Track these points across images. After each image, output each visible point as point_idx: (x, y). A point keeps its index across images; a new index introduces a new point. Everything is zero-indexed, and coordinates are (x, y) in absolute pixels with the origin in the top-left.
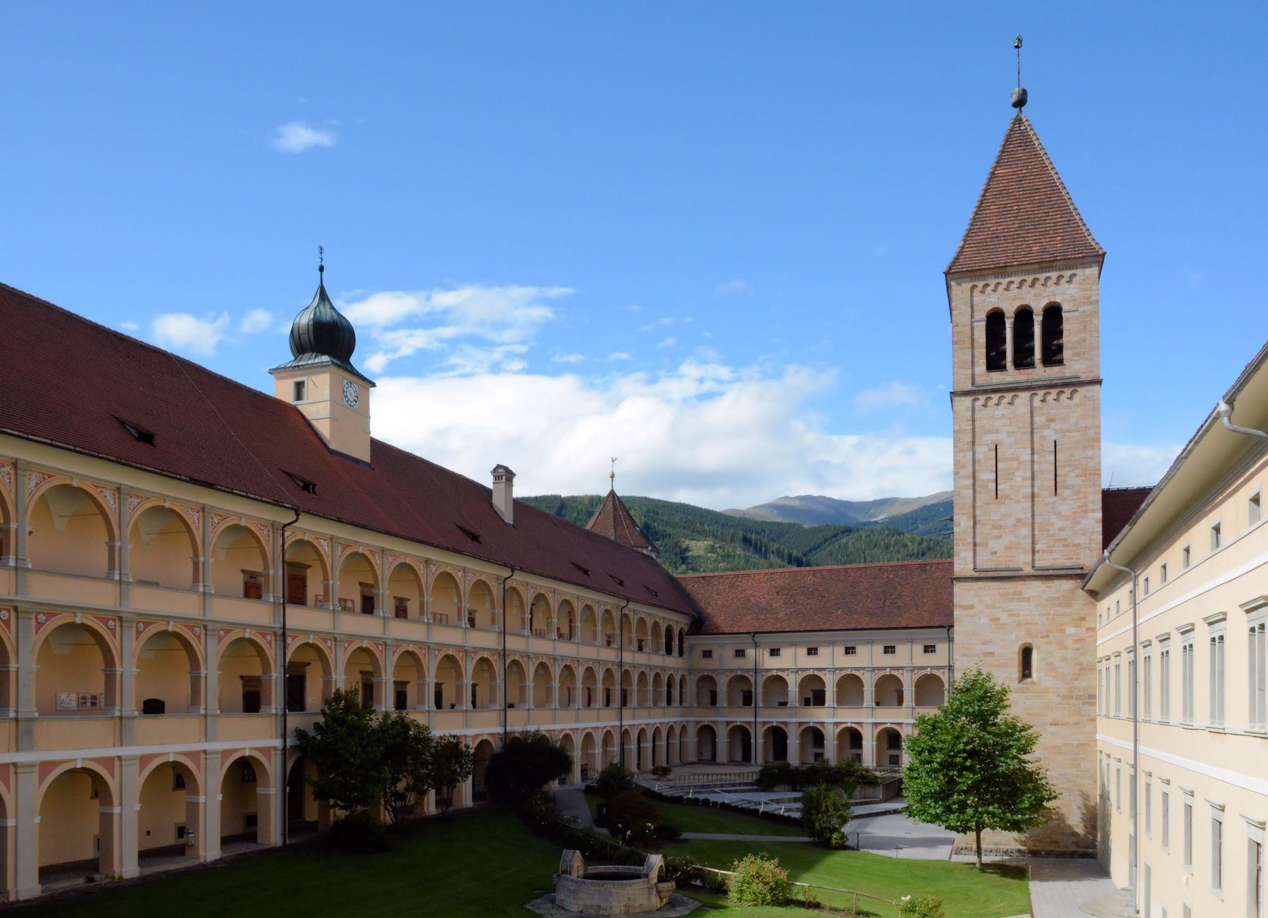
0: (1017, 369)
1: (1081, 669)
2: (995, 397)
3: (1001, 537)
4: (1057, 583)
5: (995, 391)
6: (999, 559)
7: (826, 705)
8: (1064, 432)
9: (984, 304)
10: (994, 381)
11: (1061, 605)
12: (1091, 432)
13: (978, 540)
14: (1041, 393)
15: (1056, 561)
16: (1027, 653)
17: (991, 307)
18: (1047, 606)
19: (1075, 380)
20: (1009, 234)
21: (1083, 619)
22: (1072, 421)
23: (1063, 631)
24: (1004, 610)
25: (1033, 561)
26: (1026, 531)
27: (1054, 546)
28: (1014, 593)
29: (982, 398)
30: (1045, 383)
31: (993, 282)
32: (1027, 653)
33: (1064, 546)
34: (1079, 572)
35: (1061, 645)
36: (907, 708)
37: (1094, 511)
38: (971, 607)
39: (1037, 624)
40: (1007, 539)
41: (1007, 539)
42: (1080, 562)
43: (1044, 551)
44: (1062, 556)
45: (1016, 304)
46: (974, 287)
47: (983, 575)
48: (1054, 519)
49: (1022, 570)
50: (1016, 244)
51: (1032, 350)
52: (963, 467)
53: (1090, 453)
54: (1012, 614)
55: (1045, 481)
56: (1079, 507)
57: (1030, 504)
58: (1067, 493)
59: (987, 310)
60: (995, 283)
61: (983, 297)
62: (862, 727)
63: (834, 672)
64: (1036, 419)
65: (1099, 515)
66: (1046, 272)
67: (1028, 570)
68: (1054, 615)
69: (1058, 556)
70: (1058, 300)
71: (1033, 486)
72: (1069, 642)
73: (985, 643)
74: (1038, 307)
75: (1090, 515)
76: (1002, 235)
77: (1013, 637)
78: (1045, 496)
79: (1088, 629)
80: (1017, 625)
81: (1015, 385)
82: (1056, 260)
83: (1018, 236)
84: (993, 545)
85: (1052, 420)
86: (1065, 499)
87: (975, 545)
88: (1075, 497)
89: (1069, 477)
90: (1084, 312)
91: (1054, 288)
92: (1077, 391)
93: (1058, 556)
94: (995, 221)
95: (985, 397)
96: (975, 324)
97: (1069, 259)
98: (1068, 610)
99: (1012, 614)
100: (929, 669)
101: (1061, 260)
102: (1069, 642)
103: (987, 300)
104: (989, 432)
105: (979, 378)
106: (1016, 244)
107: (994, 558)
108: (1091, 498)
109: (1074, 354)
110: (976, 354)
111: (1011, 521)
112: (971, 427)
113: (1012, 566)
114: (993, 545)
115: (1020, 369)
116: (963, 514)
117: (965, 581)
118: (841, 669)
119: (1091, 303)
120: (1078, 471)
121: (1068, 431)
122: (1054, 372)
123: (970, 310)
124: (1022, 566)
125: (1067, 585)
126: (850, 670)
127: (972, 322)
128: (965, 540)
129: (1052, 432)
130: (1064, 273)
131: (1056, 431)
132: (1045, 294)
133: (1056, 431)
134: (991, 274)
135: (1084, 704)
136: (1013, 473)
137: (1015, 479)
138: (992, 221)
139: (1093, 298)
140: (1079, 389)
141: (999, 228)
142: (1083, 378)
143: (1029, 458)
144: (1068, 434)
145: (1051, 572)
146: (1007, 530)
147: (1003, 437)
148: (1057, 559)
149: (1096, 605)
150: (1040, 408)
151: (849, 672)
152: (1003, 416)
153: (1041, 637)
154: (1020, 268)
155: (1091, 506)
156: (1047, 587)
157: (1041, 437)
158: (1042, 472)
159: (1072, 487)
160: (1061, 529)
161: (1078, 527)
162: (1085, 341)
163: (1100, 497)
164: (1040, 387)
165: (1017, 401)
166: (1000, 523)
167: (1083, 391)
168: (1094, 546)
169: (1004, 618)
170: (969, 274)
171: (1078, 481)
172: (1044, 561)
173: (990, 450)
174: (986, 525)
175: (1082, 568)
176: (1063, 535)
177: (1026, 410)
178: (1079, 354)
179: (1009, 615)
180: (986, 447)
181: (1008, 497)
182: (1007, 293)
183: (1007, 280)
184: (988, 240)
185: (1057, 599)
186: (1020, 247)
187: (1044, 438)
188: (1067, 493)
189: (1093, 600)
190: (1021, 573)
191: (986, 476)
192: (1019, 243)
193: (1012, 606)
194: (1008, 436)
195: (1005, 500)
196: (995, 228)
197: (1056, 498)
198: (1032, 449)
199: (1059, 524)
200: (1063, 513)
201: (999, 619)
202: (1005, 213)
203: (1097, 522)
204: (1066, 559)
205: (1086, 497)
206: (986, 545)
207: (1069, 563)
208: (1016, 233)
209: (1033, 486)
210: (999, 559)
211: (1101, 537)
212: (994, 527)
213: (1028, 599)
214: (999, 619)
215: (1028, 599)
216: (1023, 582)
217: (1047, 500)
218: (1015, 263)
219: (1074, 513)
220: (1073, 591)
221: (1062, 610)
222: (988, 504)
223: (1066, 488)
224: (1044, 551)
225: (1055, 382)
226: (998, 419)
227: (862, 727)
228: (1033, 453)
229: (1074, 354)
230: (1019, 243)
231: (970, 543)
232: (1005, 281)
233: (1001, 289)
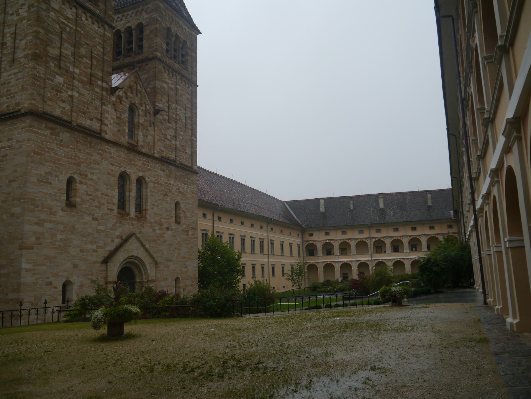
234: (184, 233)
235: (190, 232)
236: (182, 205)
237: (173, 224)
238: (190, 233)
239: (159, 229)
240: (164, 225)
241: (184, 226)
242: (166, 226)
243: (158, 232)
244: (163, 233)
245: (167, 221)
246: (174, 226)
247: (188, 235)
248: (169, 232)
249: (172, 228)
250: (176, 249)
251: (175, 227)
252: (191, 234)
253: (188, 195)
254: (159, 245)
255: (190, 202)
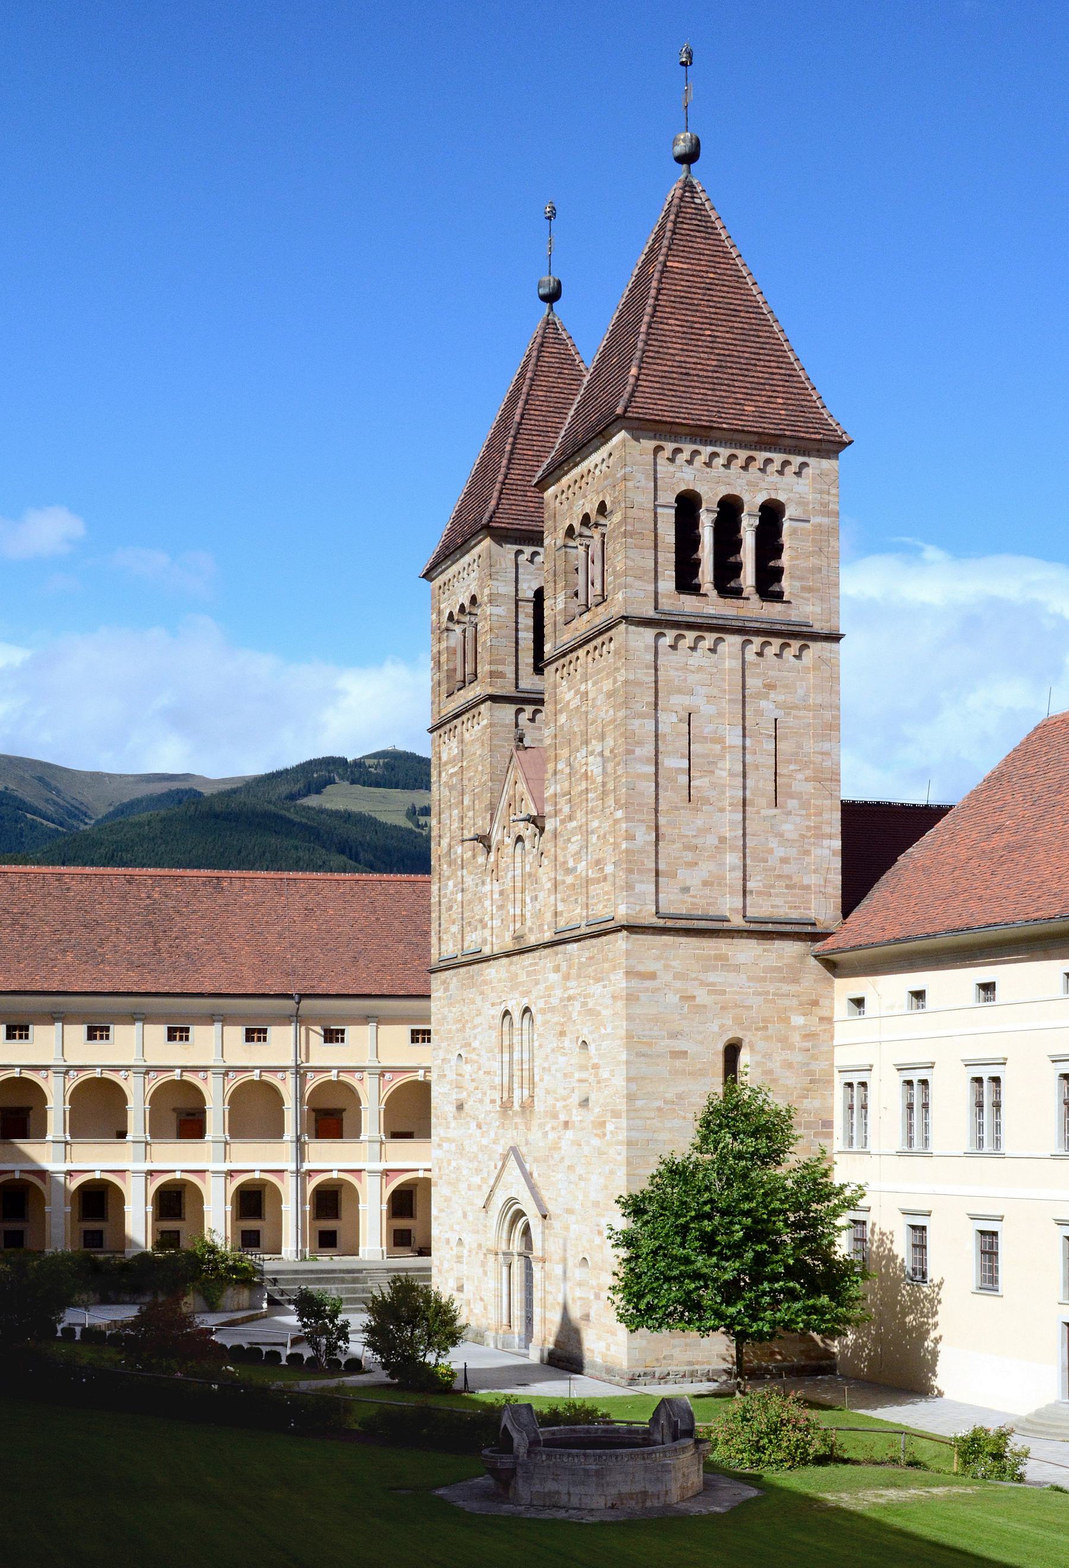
0: (721, 597)
1: (812, 1081)
2: (691, 635)
3: (696, 864)
4: (778, 944)
5: (691, 626)
6: (694, 900)
7: (49, 1137)
8: (788, 708)
9: (674, 480)
10: (688, 609)
11: (783, 980)
12: (828, 715)
13: (662, 867)
14: (758, 641)
15: (775, 910)
16: (732, 1052)
17: (683, 488)
18: (763, 979)
19: (805, 629)
20: (705, 374)
21: (815, 1003)
22: (801, 692)
23: (787, 1020)
24: (703, 984)
25: (744, 907)
26: (733, 859)
27: (773, 886)
28: (718, 957)
29: (670, 635)
30: (763, 626)
31: (688, 448)
32: (732, 1052)
33: (787, 887)
34: (809, 929)
35: (784, 1041)
36: (134, 1142)
37: (830, 837)
38: (652, 976)
39: (749, 1008)
40: (706, 869)
41: (706, 869)
42: (812, 914)
43: (759, 893)
44: (785, 902)
45: (722, 491)
46: (658, 449)
47: (670, 924)
48: (773, 843)
49: (729, 921)
50: (718, 393)
51: (738, 567)
52: (640, 743)
53: (826, 746)
54: (714, 990)
55: (760, 782)
56: (808, 828)
57: (740, 816)
58: (792, 804)
59: (678, 492)
60: (653, 447)
61: (671, 468)
62: (124, 1179)
63: (66, 1073)
64: (749, 681)
65: (837, 844)
66: (765, 450)
67: (737, 922)
68: (774, 994)
69: (779, 901)
70: (782, 497)
71: (744, 788)
72: (796, 1038)
73: (674, 1035)
74: (752, 501)
75: (826, 842)
76: (694, 372)
77: (715, 1028)
78: (761, 807)
79: (821, 1019)
80: (722, 1008)
81: (720, 622)
82: (785, 436)
83: (720, 381)
84: (685, 876)
85: (770, 687)
86: (789, 813)
87: (657, 874)
88: (804, 812)
89: (799, 782)
90: (820, 525)
91: (776, 478)
92: (808, 647)
93: (779, 901)
94: (680, 346)
95: (674, 633)
96: (660, 510)
97: (803, 438)
98: (793, 988)
99: (714, 990)
100: (257, 1071)
101: (791, 437)
102: (796, 1038)
103: (678, 475)
104: (680, 691)
105: (664, 600)
106: (718, 393)
107: (686, 897)
108: (826, 816)
109: (804, 589)
110: (659, 561)
111: (711, 840)
112: (653, 679)
113: (713, 912)
114: (685, 876)
115: (725, 598)
116: (639, 821)
117: (643, 933)
118: (80, 1068)
119: (828, 514)
120: (808, 773)
121: (796, 707)
122: (773, 611)
123: (653, 484)
124: (728, 914)
125: (792, 949)
126: (335, 1072)
127: (656, 506)
128: (643, 864)
129: (772, 706)
130: (792, 458)
131: (778, 706)
132: (764, 485)
133: (778, 706)
134: (686, 435)
135: (816, 1135)
136: (716, 763)
137: (717, 772)
138: (675, 346)
139: (832, 506)
140: (810, 643)
141: (688, 359)
142: (818, 627)
143: (739, 742)
144: (793, 712)
145: (770, 927)
146: (706, 854)
147: (698, 701)
148: (778, 906)
149: (833, 982)
150: (755, 664)
151: (97, 1074)
152: (700, 669)
153: (757, 1029)
154: (728, 435)
155: (827, 829)
156: (765, 950)
157: (755, 711)
158: (757, 767)
159: (798, 796)
160: (784, 861)
161: (807, 859)
162: (820, 570)
163: (838, 815)
164: (758, 632)
165: (722, 647)
166: (695, 841)
167: (816, 647)
168: (830, 890)
169: (702, 997)
170: (655, 427)
171: (809, 787)
172: (761, 908)
173: (680, 720)
174: (674, 842)
175: (814, 924)
176: (787, 869)
177: (737, 664)
178: (809, 590)
179: (710, 992)
180: (674, 714)
181: (707, 801)
182: (708, 470)
183: (710, 449)
184: (675, 376)
185: (779, 969)
186: (725, 400)
187: (759, 713)
188: (792, 804)
189: (829, 975)
190: (726, 925)
191: (674, 762)
192: (724, 394)
193: (712, 977)
194: (708, 701)
195: (702, 805)
196: (682, 359)
197: (774, 811)
198: (744, 728)
199: (780, 852)
200: (787, 835)
201: (694, 997)
202: (693, 337)
203: (834, 854)
204: (790, 908)
205: (820, 814)
206: (673, 875)
207: (794, 915)
208: (715, 375)
209: (744, 788)
210: (694, 900)
211: (840, 877)
212: (687, 847)
213: (737, 968)
214: (694, 997)
215: (737, 968)
216: (729, 940)
217: (764, 812)
218: (725, 426)
219: (803, 836)
220: (802, 957)
221: (785, 988)
222: (677, 808)
223: (791, 796)
224: (759, 893)
225: (778, 627)
226: (693, 672)
227: (124, 1179)
228: (744, 736)
229: (804, 589)
230: (724, 394)
231: (650, 870)
232: (707, 450)
233: (754, 467)
234: (595, 1132)
235: (607, 1125)
236: (592, 1047)
237: (574, 1111)
238: (610, 1127)
239: (553, 1128)
240: (560, 1116)
241: (597, 1110)
242: (563, 1118)
243: (552, 1136)
244: (559, 1138)
245: (564, 1103)
246: (577, 1115)
247: (604, 1135)
248: (569, 1134)
249: (574, 1122)
250: (581, 1178)
251: (579, 1118)
252: (611, 1132)
253: (605, 1012)
254: (553, 1171)
255: (609, 1030)
